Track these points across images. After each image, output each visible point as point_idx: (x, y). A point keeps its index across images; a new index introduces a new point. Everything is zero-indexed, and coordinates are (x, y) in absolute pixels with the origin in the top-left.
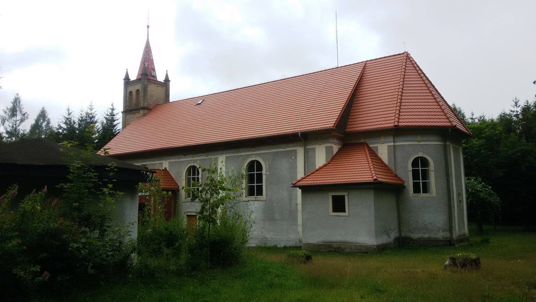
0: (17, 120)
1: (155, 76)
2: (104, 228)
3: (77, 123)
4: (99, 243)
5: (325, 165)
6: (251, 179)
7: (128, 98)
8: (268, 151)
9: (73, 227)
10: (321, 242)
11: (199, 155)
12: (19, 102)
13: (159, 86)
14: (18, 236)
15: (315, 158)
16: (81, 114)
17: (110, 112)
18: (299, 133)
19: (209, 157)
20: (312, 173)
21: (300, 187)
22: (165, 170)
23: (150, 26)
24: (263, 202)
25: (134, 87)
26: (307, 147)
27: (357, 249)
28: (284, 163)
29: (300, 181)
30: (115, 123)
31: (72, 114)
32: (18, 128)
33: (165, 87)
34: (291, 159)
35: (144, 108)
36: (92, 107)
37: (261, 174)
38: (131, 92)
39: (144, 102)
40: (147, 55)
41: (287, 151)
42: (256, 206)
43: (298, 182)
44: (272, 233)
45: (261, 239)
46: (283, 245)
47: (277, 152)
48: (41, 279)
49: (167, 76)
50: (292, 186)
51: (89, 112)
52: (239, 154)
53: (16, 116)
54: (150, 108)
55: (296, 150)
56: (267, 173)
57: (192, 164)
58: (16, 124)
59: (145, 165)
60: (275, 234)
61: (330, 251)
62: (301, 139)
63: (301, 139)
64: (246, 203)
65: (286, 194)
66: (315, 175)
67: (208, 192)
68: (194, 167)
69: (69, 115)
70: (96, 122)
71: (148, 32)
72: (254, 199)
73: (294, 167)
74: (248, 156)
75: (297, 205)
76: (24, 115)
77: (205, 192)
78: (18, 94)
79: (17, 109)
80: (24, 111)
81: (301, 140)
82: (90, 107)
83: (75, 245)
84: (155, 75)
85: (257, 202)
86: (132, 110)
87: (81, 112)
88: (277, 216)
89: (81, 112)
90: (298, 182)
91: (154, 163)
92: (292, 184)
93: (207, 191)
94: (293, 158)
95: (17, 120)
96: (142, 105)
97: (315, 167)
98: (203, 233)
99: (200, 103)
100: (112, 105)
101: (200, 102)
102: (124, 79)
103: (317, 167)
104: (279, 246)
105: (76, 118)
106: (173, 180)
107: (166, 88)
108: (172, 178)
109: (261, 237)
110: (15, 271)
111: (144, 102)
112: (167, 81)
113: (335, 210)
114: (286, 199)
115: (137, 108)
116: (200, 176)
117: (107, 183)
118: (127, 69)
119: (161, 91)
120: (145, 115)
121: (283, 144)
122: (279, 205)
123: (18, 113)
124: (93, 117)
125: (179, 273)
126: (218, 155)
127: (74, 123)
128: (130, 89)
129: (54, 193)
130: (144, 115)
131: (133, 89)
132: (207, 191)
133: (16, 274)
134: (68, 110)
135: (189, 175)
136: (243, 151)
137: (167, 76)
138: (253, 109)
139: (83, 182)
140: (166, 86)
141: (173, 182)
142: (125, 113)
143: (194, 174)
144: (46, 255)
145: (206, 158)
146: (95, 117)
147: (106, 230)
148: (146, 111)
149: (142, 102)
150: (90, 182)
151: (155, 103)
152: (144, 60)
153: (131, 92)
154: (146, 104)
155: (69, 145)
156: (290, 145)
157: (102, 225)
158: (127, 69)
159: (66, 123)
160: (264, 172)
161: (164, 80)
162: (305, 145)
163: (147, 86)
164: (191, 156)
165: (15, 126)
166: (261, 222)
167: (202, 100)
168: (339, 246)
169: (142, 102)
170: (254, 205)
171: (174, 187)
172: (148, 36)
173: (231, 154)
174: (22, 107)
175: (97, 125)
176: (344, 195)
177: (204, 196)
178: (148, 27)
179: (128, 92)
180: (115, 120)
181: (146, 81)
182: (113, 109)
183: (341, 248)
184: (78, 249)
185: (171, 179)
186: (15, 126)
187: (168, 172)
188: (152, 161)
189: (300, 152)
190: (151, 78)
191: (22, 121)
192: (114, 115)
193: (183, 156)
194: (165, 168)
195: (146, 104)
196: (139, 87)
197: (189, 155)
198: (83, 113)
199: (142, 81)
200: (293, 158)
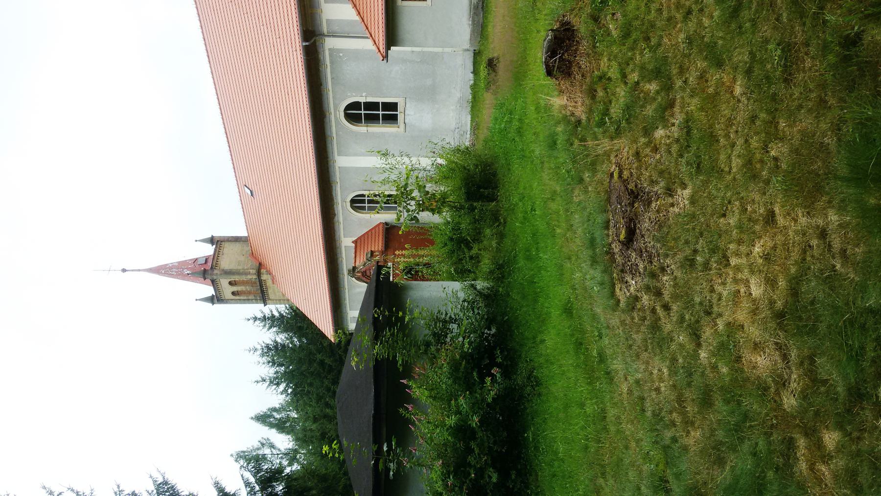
0: (271, 453)
1: (206, 259)
2: (447, 319)
3: (277, 368)
4: (465, 322)
5: (355, 6)
6: (372, 119)
7: (242, 298)
8: (331, 91)
9: (447, 350)
10: (470, 20)
11: (334, 195)
12: (244, 452)
14: (456, 400)
15: (342, 20)
16: (264, 363)
17: (259, 322)
18: (304, 44)
19: (338, 180)
20: (367, 28)
21: (388, 48)
22: (355, 242)
25: (225, 289)
26: (326, 34)
29: (378, 49)
30: (276, 314)
31: (263, 376)
32: (283, 450)
33: (223, 243)
35: (259, 274)
37: (366, 104)
38: (233, 293)
39: (249, 273)
41: (332, 63)
42: (412, 113)
43: (379, 51)
46: (472, 75)
47: (332, 78)
48: (498, 375)
49: (204, 241)
50: (385, 61)
51: (259, 352)
52: (334, 135)
53: (265, 454)
54: (258, 265)
55: (330, 49)
56: (364, 95)
57: (349, 204)
58: (278, 454)
59: (349, 271)
60: (454, 86)
61: (482, 8)
62: (312, 41)
63: (312, 41)
66: (369, 25)
67: (408, 202)
68: (353, 201)
69: (265, 381)
70: (276, 342)
71: (133, 270)
73: (357, 55)
74: (338, 122)
76: (263, 444)
77: (409, 206)
78: (232, 455)
79: (255, 454)
80: (257, 444)
81: (315, 42)
82: (252, 352)
83: (467, 346)
84: (205, 258)
85: (406, 111)
86: (261, 290)
87: (261, 364)
88: (429, 82)
90: (379, 51)
91: (344, 258)
92: (383, 60)
93: (407, 204)
95: (271, 453)
96: (255, 277)
97: (356, 21)
98: (455, 207)
99: (251, 192)
101: (249, 192)
102: (213, 303)
103: (357, 18)
104: (472, 82)
105: (270, 371)
106: (371, 230)
107: (224, 241)
108: (367, 233)
109: (458, 107)
110: (490, 400)
111: (249, 273)
112: (212, 240)
114: (403, 68)
115: (258, 283)
116: (366, 193)
117: (397, 318)
118: (197, 300)
119: (229, 250)
120: (269, 273)
123: (261, 452)
124: (267, 347)
125: (501, 236)
126: (334, 167)
127: (277, 372)
129: (408, 372)
130: (270, 274)
131: (227, 290)
132: (407, 204)
133: (493, 399)
134: (258, 382)
135: (363, 208)
137: (204, 241)
138: (261, 111)
139: (397, 342)
140: (222, 242)
141: (373, 231)
143: (363, 201)
144: (475, 374)
145: (339, 183)
147: (450, 317)
148: (262, 270)
149: (249, 277)
150: (397, 335)
151: (250, 258)
152: (179, 275)
153: (233, 293)
154: (251, 271)
155: (356, 359)
157: (445, 322)
158: (197, 300)
159: (278, 384)
160: (362, 100)
161: (211, 245)
162: (321, 35)
163: (223, 270)
164: (335, 206)
165: (281, 455)
166: (437, 106)
167: (246, 188)
169: (249, 277)
171: (381, 230)
173: (335, 147)
174: (252, 448)
175: (279, 340)
177: (414, 207)
180: (273, 315)
181: (216, 272)
182: (255, 319)
184: (470, 343)
185: (370, 233)
186: (281, 455)
187: (360, 238)
189: (330, 43)
190: (210, 264)
191: (272, 446)
192: (265, 316)
193: (336, 219)
194: (353, 242)
195: (251, 271)
196: (224, 282)
197: (333, 209)
198: (262, 362)
199: (215, 277)
200: (341, 55)
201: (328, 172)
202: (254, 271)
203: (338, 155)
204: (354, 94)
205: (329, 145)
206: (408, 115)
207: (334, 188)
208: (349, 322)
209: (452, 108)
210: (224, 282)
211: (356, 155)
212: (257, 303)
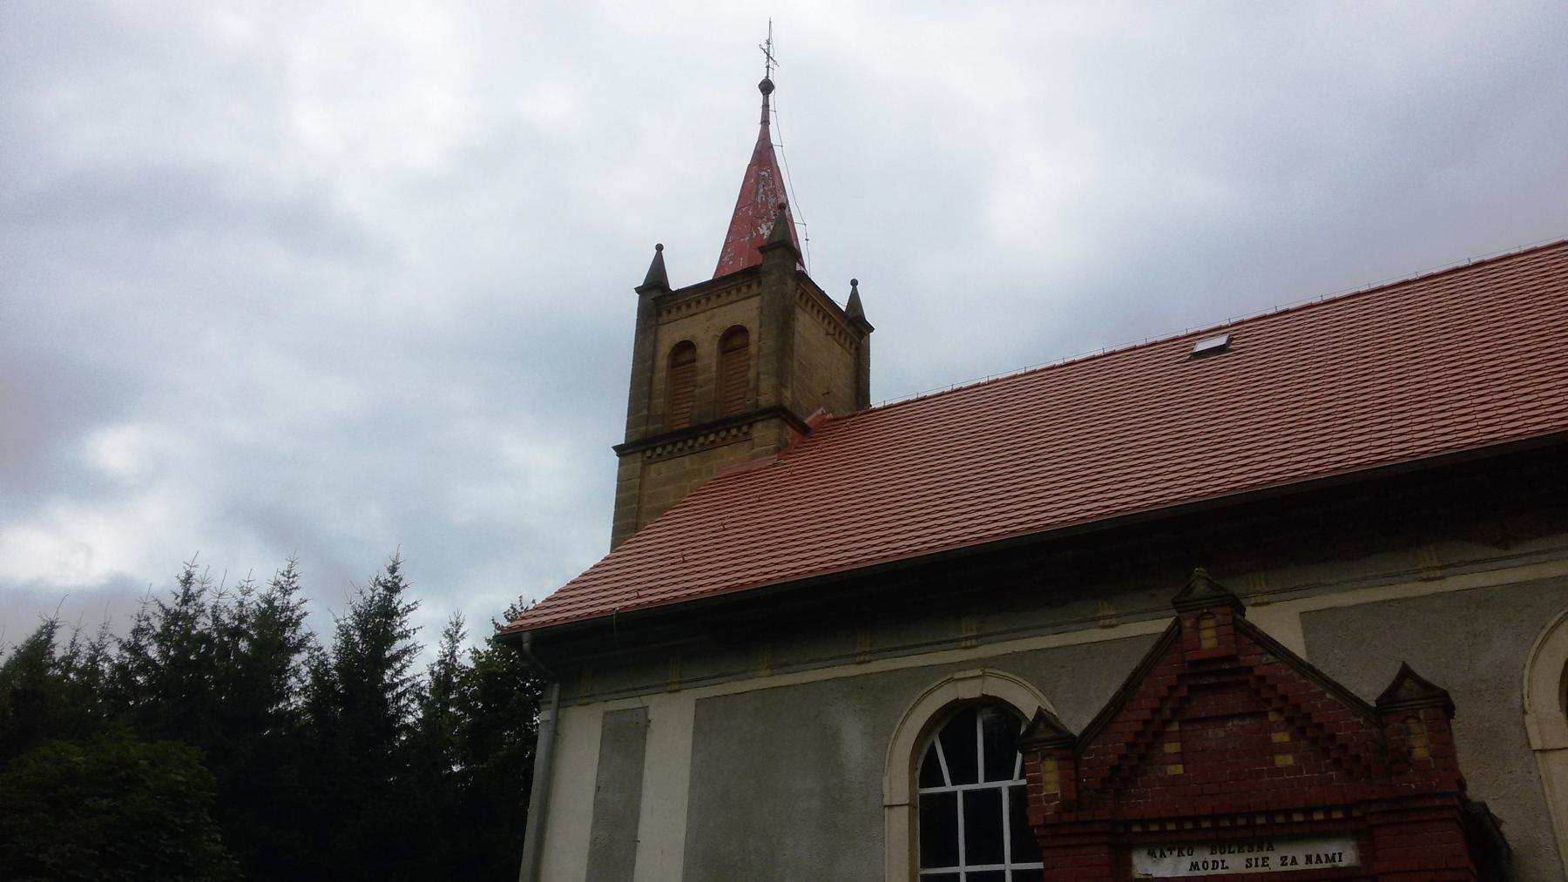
7: (661, 374)
13: (831, 330)
16: (241, 604)
23: (775, 83)
25: (709, 319)
33: (853, 351)
35: (781, 413)
36: (291, 580)
40: (765, 192)
69: (185, 602)
70: (299, 647)
71: (766, 106)
82: (283, 579)
87: (240, 597)
89: (240, 597)
96: (767, 399)
100: (393, 570)
120: (782, 449)
128: (671, 335)
130: (778, 450)
142: (644, 452)
146: (297, 623)
149: (767, 384)
153: (685, 348)
172: (765, 122)
175: (297, 659)
178: (767, 87)
179: (665, 347)
182: (393, 589)
188: (1093, 621)
198: (248, 600)
202: (787, 403)
208: (613, 706)
210: (745, 311)
212: (631, 425)
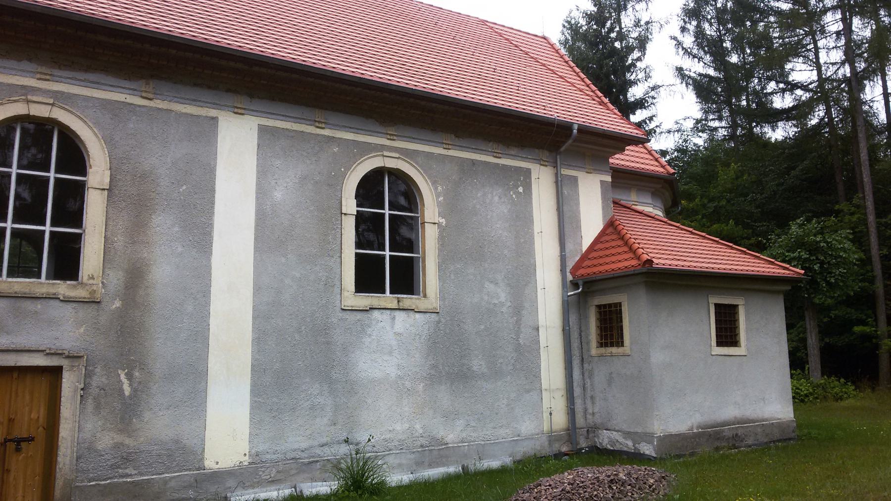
10: (698, 427)
11: (91, 76)
15: (578, 204)
18: (576, 127)
24: (429, 314)
27: (767, 435)
28: (496, 198)
34: (514, 193)
41: (504, 167)
44: (460, 423)
45: (422, 446)
47: (473, 162)
52: (327, 132)
56: (443, 221)
64: (359, 316)
65: (503, 299)
72: (394, 305)
74: (367, 149)
75: (538, 329)
88: (478, 364)
94: (521, 189)
109: (423, 441)
113: (720, 344)
114: (504, 309)
121: (490, 141)
122: (482, 327)
136: (345, 127)
156: (513, 152)
164: (26, 65)
166: (421, 387)
168: (735, 433)
170: (393, 327)
176: (738, 305)
183: (739, 437)
200: (521, 189)
201: (195, 85)
203: (262, 129)
204: (441, 199)
205: (296, 111)
206: (394, 318)
207: (133, 85)
209: (418, 426)
211: (262, 172)
